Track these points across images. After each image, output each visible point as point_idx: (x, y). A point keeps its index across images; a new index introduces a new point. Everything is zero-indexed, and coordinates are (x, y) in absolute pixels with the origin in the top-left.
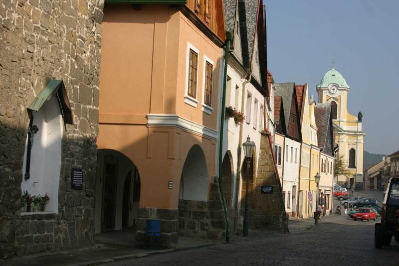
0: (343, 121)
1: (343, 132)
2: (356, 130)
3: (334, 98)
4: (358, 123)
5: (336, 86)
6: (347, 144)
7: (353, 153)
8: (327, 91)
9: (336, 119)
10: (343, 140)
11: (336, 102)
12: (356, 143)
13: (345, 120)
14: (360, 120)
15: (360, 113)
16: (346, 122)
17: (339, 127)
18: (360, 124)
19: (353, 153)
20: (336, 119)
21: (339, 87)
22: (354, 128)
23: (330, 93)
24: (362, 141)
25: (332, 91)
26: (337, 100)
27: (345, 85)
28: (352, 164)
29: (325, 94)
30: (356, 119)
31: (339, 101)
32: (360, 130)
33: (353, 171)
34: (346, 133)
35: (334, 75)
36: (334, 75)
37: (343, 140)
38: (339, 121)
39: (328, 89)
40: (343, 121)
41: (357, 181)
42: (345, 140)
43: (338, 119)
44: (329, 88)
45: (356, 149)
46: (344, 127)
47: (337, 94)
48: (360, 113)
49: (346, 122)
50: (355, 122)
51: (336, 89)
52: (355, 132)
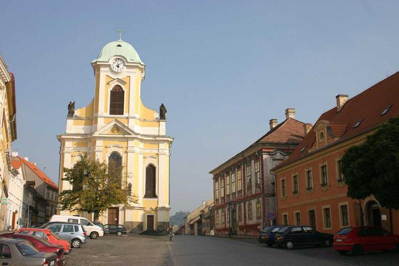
0: (134, 118)
1: (133, 136)
2: (157, 134)
3: (119, 80)
4: (159, 121)
5: (121, 58)
7: (151, 171)
8: (107, 69)
9: (123, 114)
10: (135, 149)
11: (123, 86)
12: (157, 154)
13: (138, 116)
14: (162, 117)
15: (162, 105)
16: (140, 119)
17: (128, 128)
18: (163, 124)
19: (151, 171)
20: (123, 114)
21: (128, 62)
22: (152, 130)
23: (112, 71)
24: (167, 152)
25: (116, 69)
26: (124, 83)
27: (137, 59)
28: (151, 191)
29: (104, 73)
30: (157, 115)
31: (127, 85)
32: (163, 133)
33: (151, 203)
34: (139, 137)
35: (119, 46)
36: (119, 46)
37: (135, 149)
38: (128, 118)
39: (109, 66)
40: (134, 118)
41: (159, 221)
42: (137, 150)
43: (125, 114)
44: (111, 62)
45: (156, 165)
46: (135, 126)
47: (124, 73)
48: (162, 105)
49: (140, 119)
50: (154, 121)
51: (121, 66)
52: (155, 136)
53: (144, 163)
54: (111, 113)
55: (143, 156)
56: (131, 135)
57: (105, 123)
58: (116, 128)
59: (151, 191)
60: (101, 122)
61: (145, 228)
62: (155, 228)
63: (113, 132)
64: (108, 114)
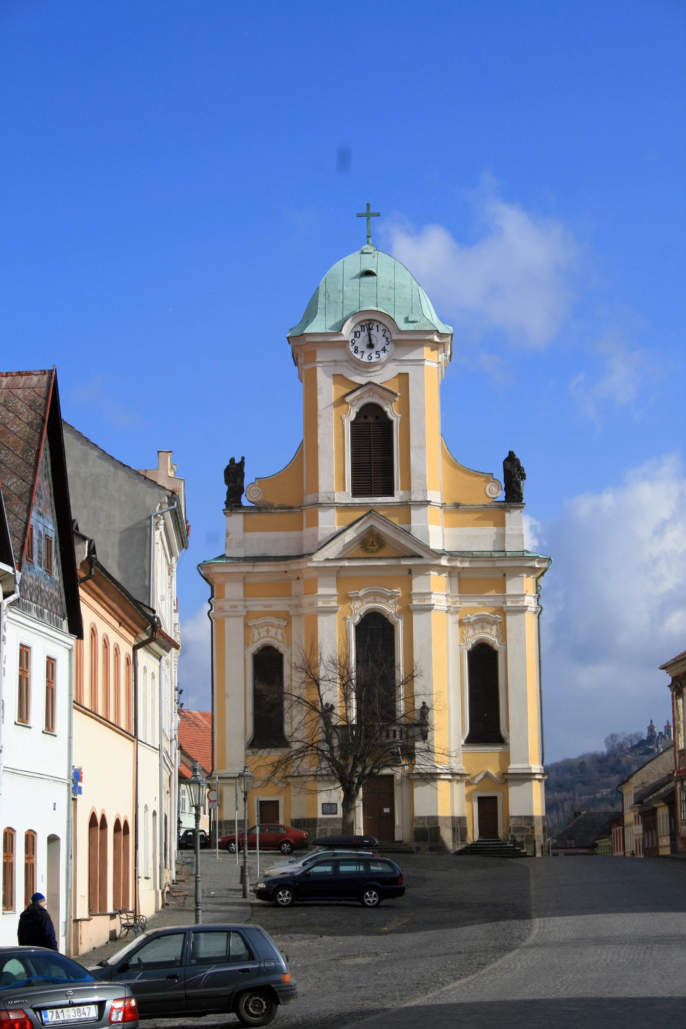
6: (453, 619)
9: (392, 495)
15: (511, 454)
20: (392, 495)
24: (530, 601)
28: (486, 722)
34: (444, 562)
43: (399, 495)
46: (436, 532)
53: (462, 639)
54: (355, 494)
55: (457, 617)
56: (420, 557)
57: (339, 524)
58: (371, 543)
59: (486, 722)
60: (328, 522)
61: (473, 834)
62: (501, 833)
63: (366, 550)
64: (346, 496)
